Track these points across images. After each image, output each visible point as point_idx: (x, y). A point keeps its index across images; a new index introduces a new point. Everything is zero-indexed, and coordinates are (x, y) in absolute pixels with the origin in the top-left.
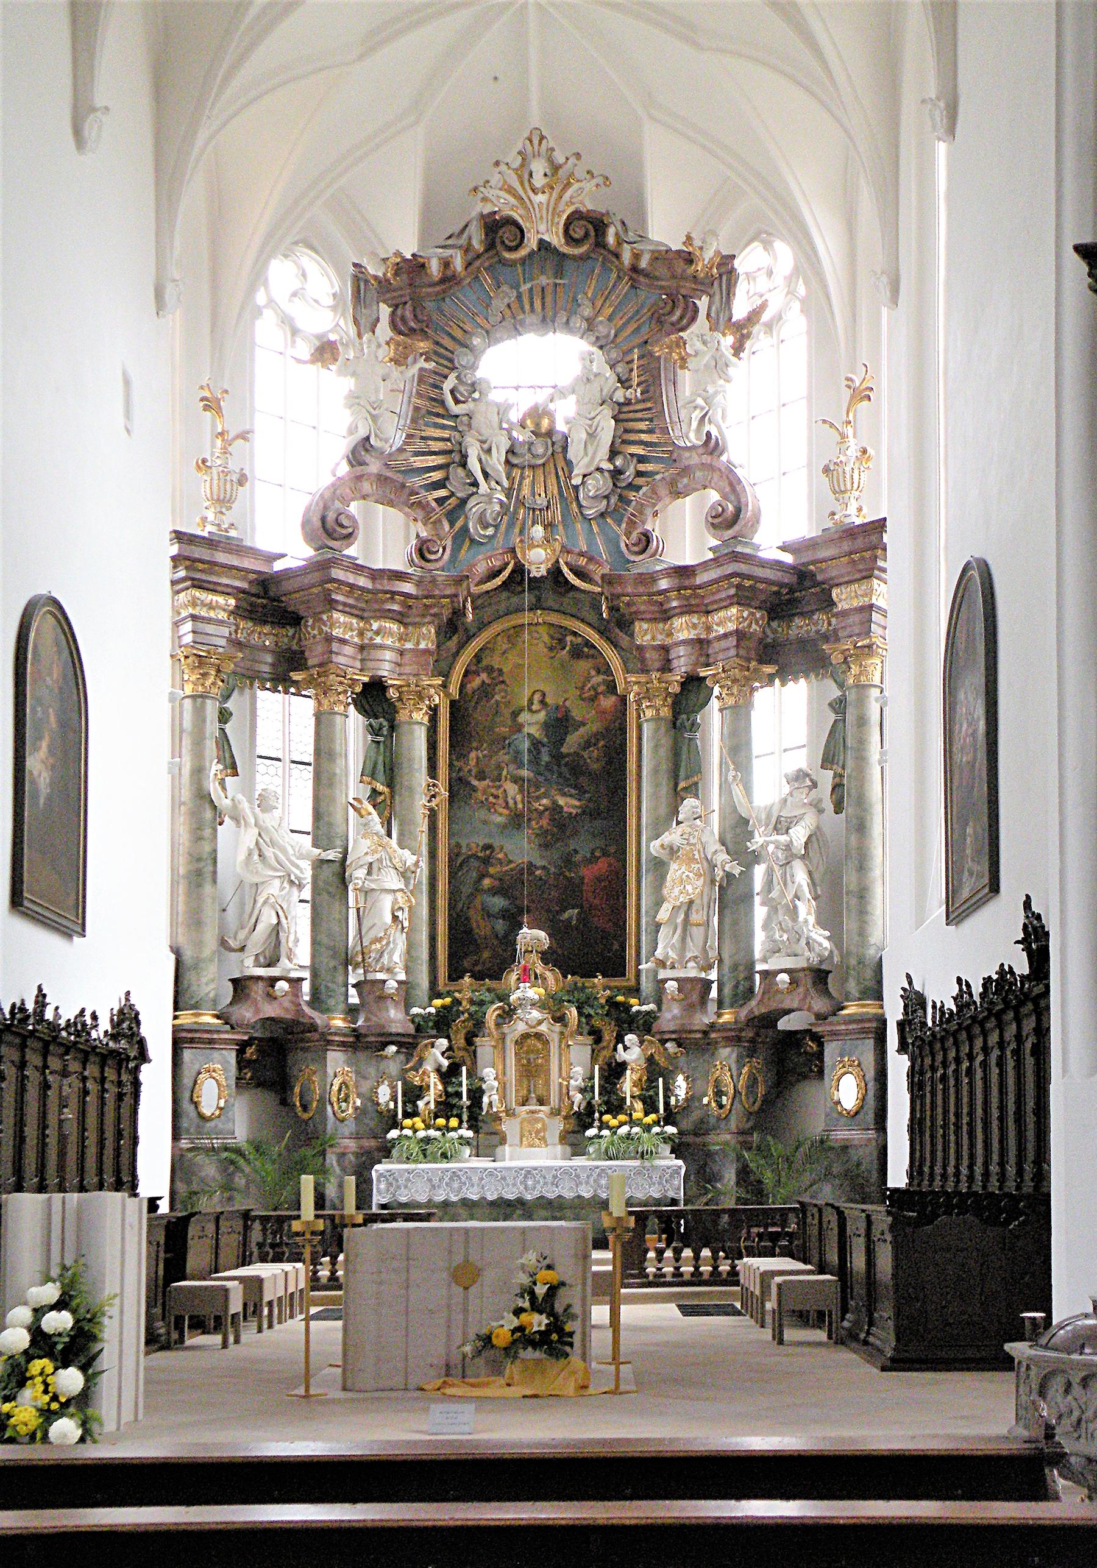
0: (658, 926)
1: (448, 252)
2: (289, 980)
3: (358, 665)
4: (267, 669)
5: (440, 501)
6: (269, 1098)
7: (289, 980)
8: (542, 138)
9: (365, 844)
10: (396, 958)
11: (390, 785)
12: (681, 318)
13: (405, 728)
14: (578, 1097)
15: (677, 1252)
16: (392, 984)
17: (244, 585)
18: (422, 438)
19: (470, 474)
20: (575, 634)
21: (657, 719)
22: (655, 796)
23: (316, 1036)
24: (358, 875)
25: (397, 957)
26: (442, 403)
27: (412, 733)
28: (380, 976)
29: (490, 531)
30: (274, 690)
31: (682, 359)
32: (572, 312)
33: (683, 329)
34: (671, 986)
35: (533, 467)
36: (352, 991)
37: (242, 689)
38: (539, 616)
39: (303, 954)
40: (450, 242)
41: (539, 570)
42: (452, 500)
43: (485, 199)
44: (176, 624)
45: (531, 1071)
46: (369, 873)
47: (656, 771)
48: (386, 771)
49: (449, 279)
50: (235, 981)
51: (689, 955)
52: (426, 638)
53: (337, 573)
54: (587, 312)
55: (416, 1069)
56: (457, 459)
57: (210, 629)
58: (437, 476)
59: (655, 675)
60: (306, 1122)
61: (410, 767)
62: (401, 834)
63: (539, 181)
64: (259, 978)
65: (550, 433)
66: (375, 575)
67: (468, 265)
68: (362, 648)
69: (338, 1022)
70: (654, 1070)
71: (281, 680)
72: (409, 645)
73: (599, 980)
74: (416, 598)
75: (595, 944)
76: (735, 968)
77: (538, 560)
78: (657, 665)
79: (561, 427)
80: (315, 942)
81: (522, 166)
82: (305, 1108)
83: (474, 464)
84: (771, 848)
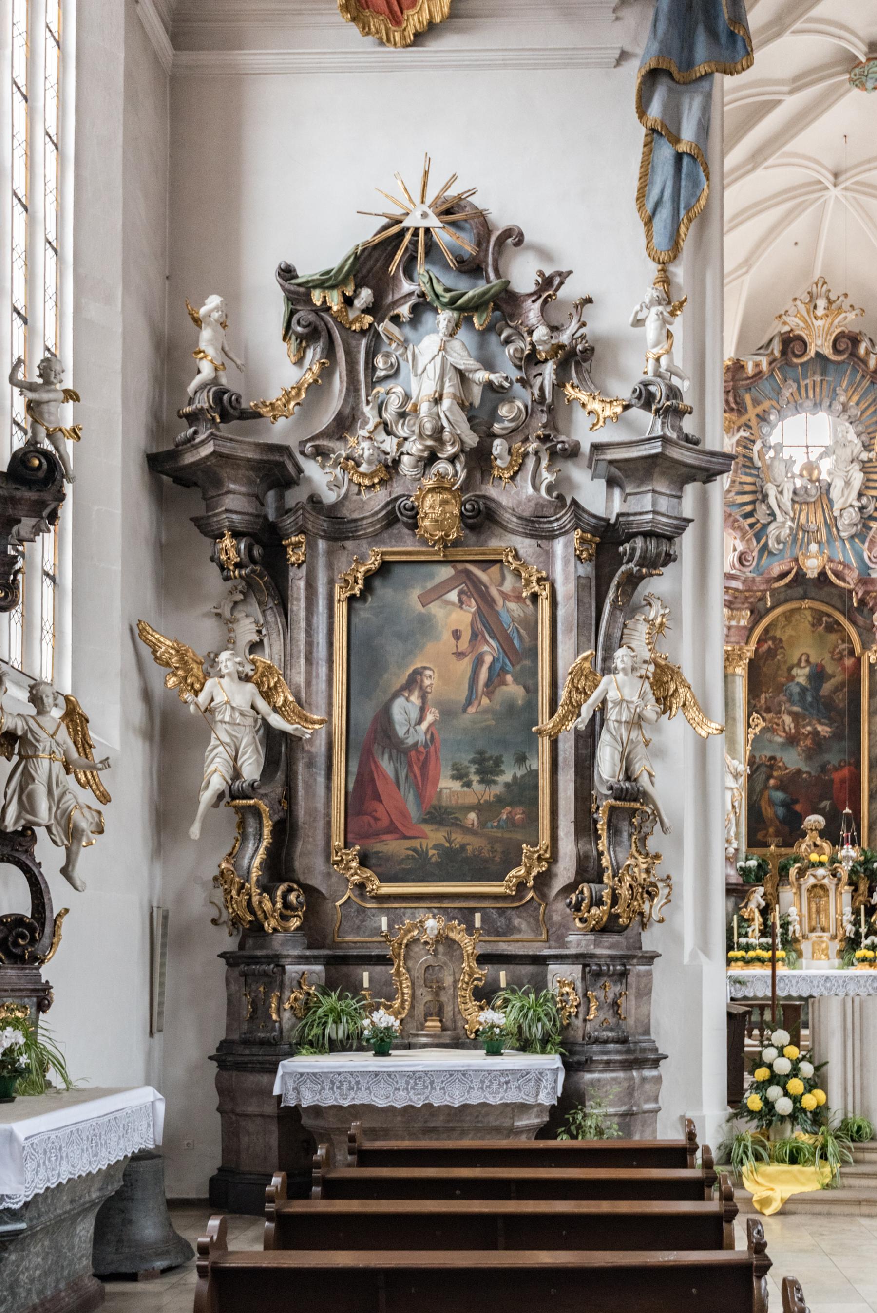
1: (758, 358)
5: (752, 526)
8: (825, 283)
18: (741, 483)
19: (769, 507)
20: (829, 616)
26: (751, 459)
29: (781, 546)
32: (832, 400)
35: (808, 503)
40: (761, 351)
41: (812, 574)
42: (758, 526)
43: (785, 323)
49: (758, 374)
54: (843, 399)
56: (760, 497)
58: (749, 508)
63: (820, 312)
65: (818, 480)
67: (770, 363)
74: (741, 591)
77: (812, 566)
79: (824, 476)
81: (810, 301)
83: (772, 501)
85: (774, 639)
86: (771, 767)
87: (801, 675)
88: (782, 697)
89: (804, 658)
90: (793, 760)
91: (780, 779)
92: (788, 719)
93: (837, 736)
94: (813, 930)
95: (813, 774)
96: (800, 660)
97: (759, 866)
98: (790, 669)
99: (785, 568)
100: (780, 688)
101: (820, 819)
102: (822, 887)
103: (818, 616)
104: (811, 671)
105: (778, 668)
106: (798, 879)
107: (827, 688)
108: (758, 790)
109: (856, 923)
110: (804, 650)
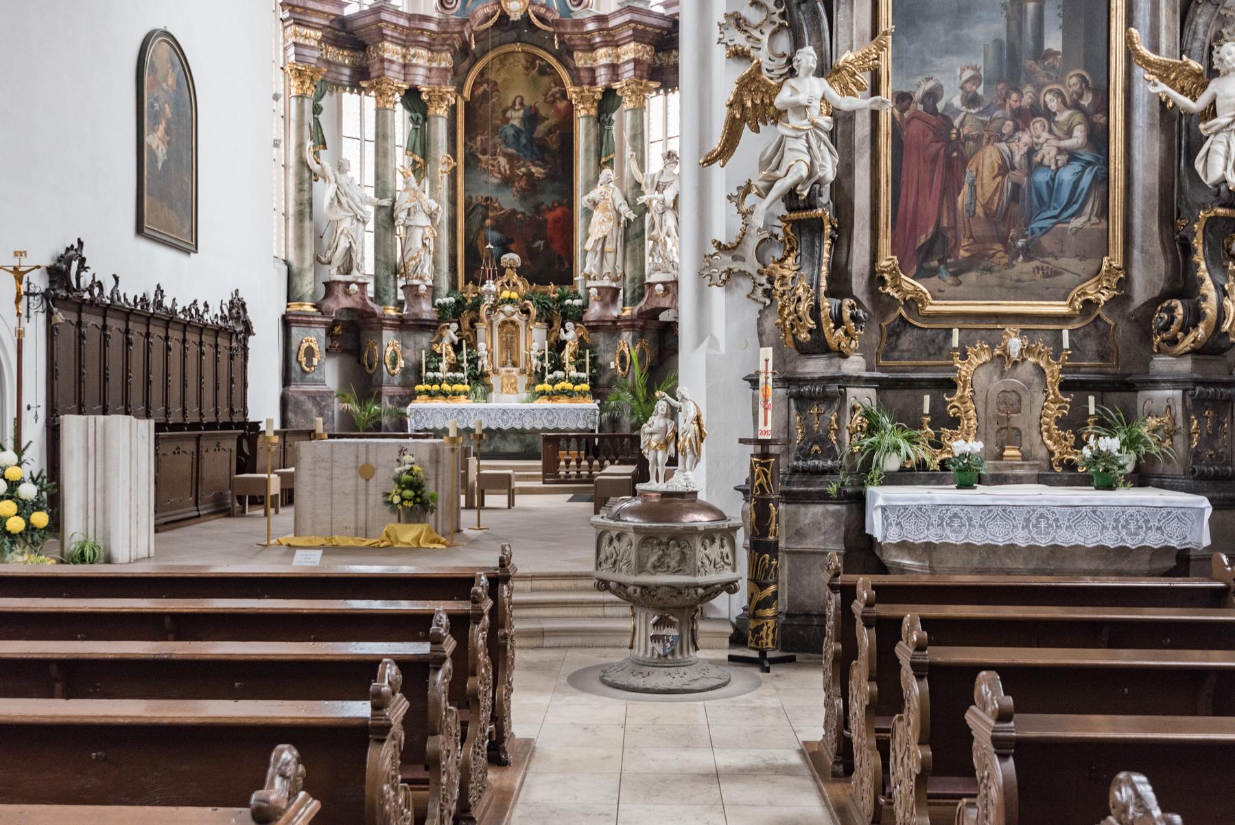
0: (586, 252)
2: (358, 284)
3: (402, 77)
4: (345, 79)
6: (350, 360)
7: (358, 284)
9: (406, 195)
10: (426, 271)
11: (424, 156)
13: (432, 119)
14: (535, 361)
15: (591, 462)
16: (423, 288)
17: (327, 23)
21: (588, 116)
22: (587, 167)
23: (375, 320)
24: (401, 216)
25: (427, 271)
27: (436, 123)
28: (416, 282)
30: (352, 92)
34: (593, 291)
36: (400, 292)
37: (331, 92)
38: (518, 47)
39: (369, 267)
44: (285, 49)
45: (509, 346)
46: (409, 215)
47: (587, 150)
48: (421, 146)
50: (326, 284)
51: (605, 271)
52: (446, 60)
53: (385, 16)
55: (438, 342)
57: (306, 52)
59: (586, 87)
60: (371, 376)
61: (436, 145)
62: (431, 189)
64: (339, 282)
66: (411, 17)
68: (405, 66)
69: (391, 311)
70: (582, 343)
71: (355, 86)
72: (435, 65)
73: (552, 287)
75: (551, 261)
76: (633, 280)
78: (587, 81)
80: (376, 260)
82: (371, 366)
84: (654, 202)
85: (487, 81)
86: (487, 208)
87: (516, 117)
88: (498, 140)
89: (518, 101)
90: (508, 201)
91: (496, 219)
92: (503, 161)
93: (551, 178)
94: (504, 365)
95: (528, 214)
96: (514, 103)
97: (457, 302)
98: (505, 111)
99: (488, 10)
100: (496, 130)
101: (516, 257)
102: (513, 323)
103: (532, 59)
104: (525, 114)
105: (493, 111)
106: (488, 316)
107: (541, 129)
108: (474, 229)
109: (542, 359)
110: (517, 94)
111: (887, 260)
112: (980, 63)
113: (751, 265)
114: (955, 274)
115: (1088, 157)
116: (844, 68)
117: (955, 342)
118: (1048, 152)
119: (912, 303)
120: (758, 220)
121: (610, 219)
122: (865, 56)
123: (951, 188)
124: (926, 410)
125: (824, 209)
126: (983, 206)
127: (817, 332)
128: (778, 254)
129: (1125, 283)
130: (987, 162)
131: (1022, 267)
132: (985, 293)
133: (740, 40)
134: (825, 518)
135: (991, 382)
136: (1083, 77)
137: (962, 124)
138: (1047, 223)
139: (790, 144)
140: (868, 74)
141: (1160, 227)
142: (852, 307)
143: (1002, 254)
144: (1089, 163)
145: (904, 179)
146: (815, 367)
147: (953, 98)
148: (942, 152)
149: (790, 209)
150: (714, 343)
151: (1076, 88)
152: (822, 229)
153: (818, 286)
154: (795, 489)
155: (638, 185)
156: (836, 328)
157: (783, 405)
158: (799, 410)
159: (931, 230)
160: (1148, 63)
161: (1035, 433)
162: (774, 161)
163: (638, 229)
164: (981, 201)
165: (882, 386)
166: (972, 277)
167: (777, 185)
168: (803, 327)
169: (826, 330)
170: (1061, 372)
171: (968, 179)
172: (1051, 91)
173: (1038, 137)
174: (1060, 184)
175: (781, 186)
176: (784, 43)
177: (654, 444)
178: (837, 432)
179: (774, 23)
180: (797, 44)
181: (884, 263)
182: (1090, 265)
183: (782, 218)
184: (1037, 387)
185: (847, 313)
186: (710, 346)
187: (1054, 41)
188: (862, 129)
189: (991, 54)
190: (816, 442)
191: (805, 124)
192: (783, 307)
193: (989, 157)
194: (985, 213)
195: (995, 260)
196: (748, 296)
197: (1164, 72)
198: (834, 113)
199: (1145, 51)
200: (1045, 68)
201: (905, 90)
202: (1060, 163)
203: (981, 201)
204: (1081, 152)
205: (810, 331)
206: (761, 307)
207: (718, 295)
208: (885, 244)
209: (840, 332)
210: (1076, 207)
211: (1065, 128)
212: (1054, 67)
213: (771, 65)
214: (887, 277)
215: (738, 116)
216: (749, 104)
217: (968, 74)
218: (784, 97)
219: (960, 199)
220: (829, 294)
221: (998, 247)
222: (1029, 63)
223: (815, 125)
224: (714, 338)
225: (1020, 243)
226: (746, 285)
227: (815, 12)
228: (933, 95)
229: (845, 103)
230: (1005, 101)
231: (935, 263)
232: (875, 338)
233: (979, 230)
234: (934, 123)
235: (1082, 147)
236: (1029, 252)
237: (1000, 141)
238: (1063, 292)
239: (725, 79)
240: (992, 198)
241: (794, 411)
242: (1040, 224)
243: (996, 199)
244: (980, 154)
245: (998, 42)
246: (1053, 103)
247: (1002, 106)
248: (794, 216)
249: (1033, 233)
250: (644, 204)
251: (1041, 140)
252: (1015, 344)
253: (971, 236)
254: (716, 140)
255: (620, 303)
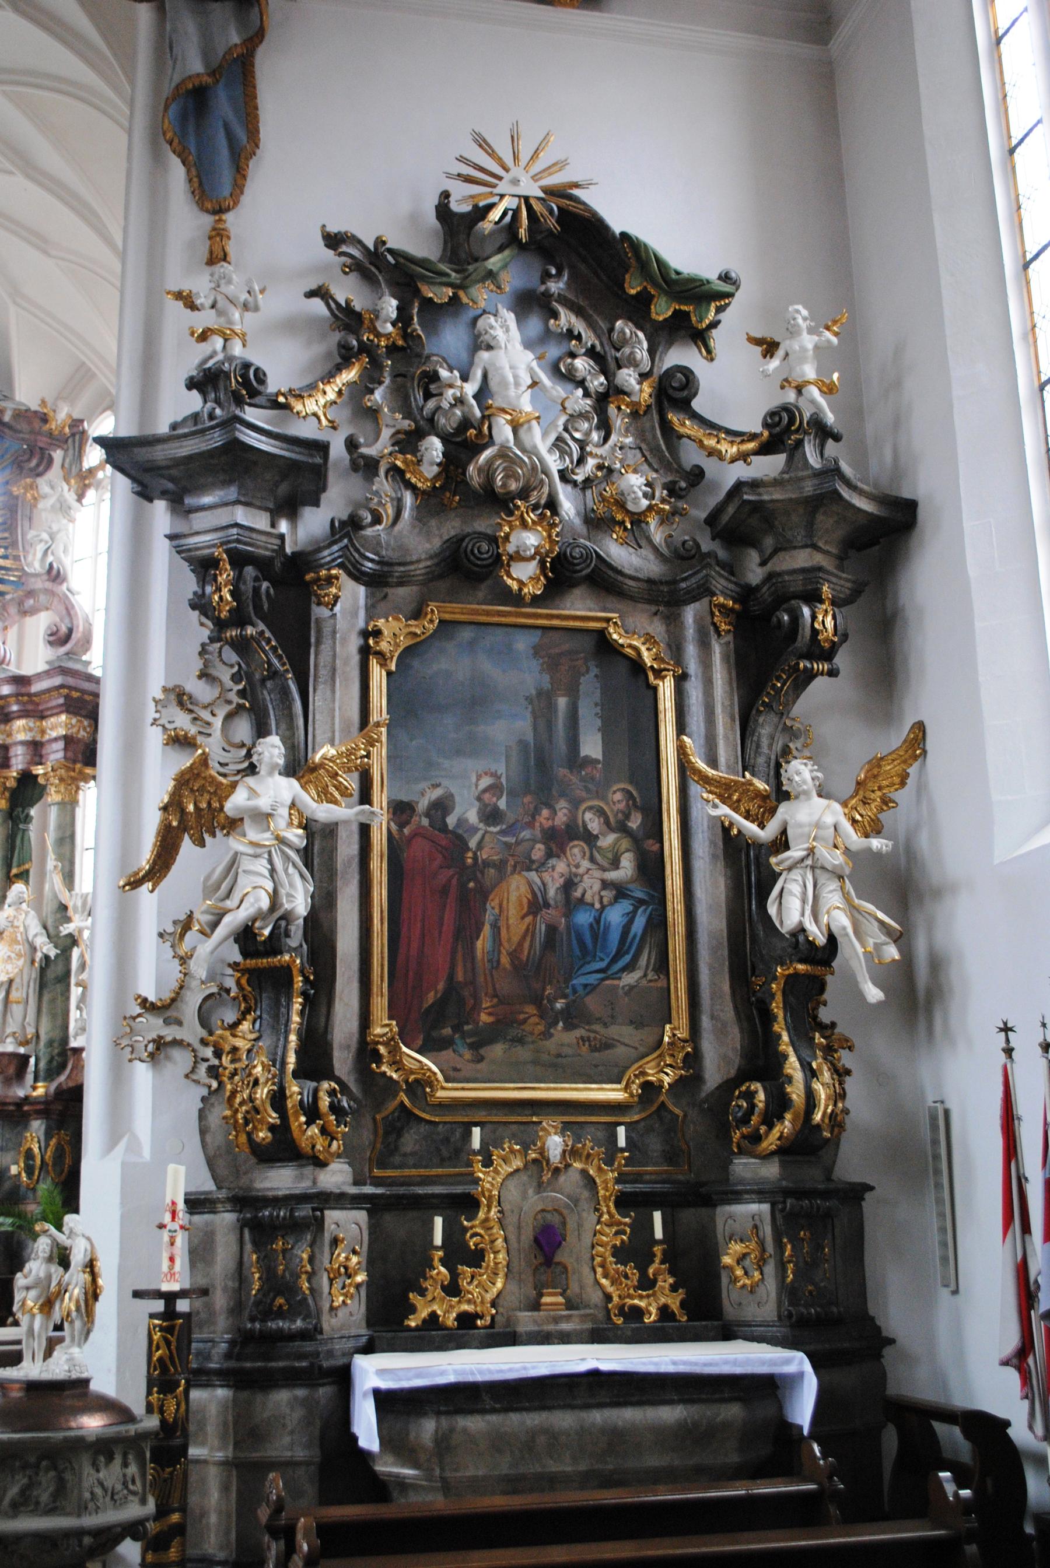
12: (38, 465)
31: (35, 499)
33: (39, 475)
51: (9, 1031)
111: (382, 1027)
112: (502, 770)
113: (191, 1031)
114: (475, 1047)
115: (639, 894)
116: (321, 765)
117: (476, 1143)
118: (590, 886)
119: (419, 1086)
120: (199, 969)
121: (19, 955)
122: (350, 753)
123: (467, 929)
124: (438, 1240)
125: (293, 956)
126: (510, 954)
127: (282, 1129)
128: (230, 1017)
129: (693, 1060)
130: (513, 897)
131: (563, 1037)
132: (517, 1074)
133: (182, 721)
134: (292, 1409)
135: (524, 1196)
136: (628, 792)
137: (480, 845)
138: (592, 979)
139: (246, 864)
140: (356, 775)
141: (732, 987)
142: (332, 1093)
143: (534, 1020)
144: (641, 902)
145: (405, 915)
146: (281, 1180)
147: (466, 811)
148: (454, 881)
149: (245, 954)
150: (134, 1147)
151: (622, 806)
152: (290, 982)
153: (284, 1063)
154: (248, 1365)
155: (64, 908)
156: (309, 1123)
157: (233, 1239)
158: (257, 1245)
159: (441, 986)
160: (705, 780)
161: (586, 1270)
162: (224, 887)
163: (59, 969)
164: (507, 947)
165: (374, 1206)
166: (497, 1050)
167: (227, 919)
168: (262, 1121)
169: (294, 1126)
170: (618, 1181)
171: (489, 917)
172: (590, 808)
173: (577, 866)
174: (607, 927)
175: (232, 921)
176: (243, 729)
177: (30, 1303)
178: (311, 1276)
179: (229, 702)
180: (261, 731)
181: (378, 1030)
182: (647, 1035)
183: (235, 966)
184: (585, 1205)
185: (325, 1102)
186: (128, 1149)
187: (592, 747)
188: (347, 848)
189: (514, 753)
190: (279, 1293)
191: (266, 838)
192: (234, 1093)
193: (516, 889)
194: (512, 963)
195: (527, 1027)
196: (187, 1076)
197: (725, 791)
198: (308, 826)
199: (701, 765)
200: (583, 780)
201: (405, 799)
202: (605, 901)
203: (507, 947)
204: (630, 886)
205: (272, 1128)
206: (205, 1092)
207: (142, 1074)
208: (380, 1004)
209: (314, 1130)
210: (627, 958)
211: (610, 855)
212: (593, 779)
213: (225, 758)
214: (382, 1049)
215: (175, 824)
216: (191, 808)
217: (486, 782)
218: (238, 801)
219: (479, 944)
220: (296, 1075)
221: (531, 1009)
222: (562, 772)
223: (281, 840)
224: (135, 1138)
225: (559, 1005)
226: (182, 1060)
227: (285, 692)
228: (441, 807)
229: (323, 812)
230: (533, 817)
231: (447, 1031)
232: (367, 1136)
233: (506, 986)
234: (443, 843)
235: (632, 881)
236: (572, 1017)
237: (529, 870)
238: (616, 1070)
239: (159, 774)
240: (520, 944)
241: (248, 1247)
242: (583, 980)
243: (527, 945)
244: (504, 884)
245: (523, 744)
246: (594, 825)
247: (531, 825)
248: (251, 963)
249: (575, 991)
250: (70, 935)
251: (581, 871)
252: (555, 1144)
253: (495, 995)
254: (145, 857)
255: (29, 1077)
